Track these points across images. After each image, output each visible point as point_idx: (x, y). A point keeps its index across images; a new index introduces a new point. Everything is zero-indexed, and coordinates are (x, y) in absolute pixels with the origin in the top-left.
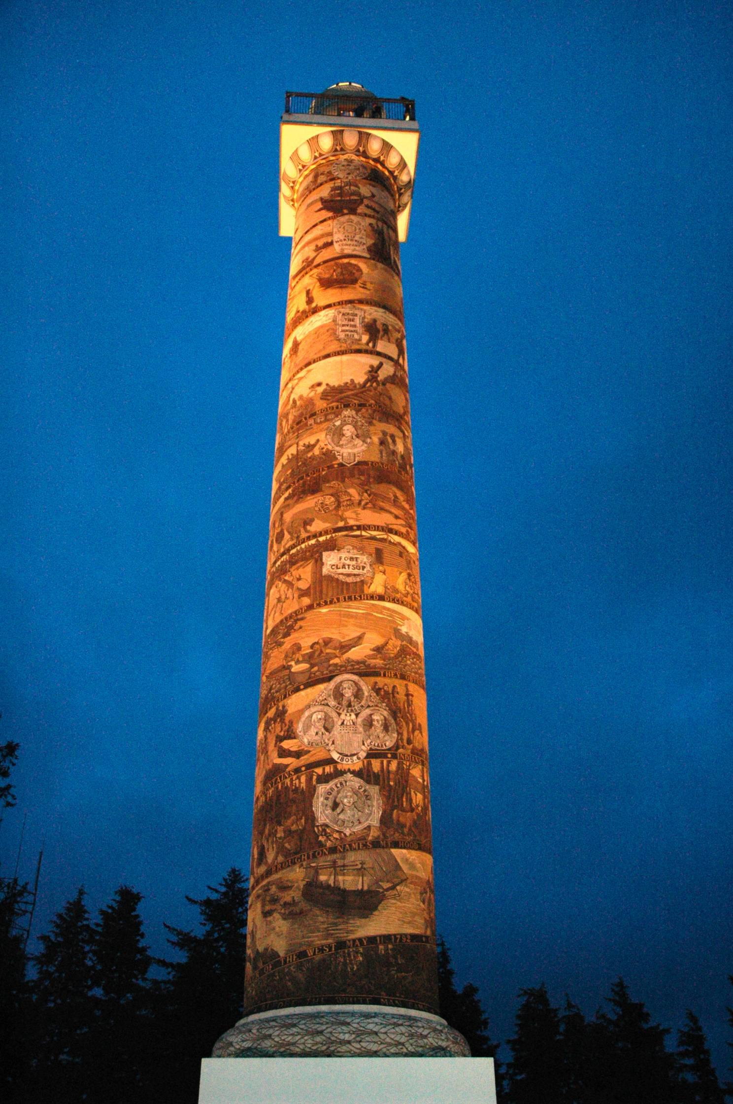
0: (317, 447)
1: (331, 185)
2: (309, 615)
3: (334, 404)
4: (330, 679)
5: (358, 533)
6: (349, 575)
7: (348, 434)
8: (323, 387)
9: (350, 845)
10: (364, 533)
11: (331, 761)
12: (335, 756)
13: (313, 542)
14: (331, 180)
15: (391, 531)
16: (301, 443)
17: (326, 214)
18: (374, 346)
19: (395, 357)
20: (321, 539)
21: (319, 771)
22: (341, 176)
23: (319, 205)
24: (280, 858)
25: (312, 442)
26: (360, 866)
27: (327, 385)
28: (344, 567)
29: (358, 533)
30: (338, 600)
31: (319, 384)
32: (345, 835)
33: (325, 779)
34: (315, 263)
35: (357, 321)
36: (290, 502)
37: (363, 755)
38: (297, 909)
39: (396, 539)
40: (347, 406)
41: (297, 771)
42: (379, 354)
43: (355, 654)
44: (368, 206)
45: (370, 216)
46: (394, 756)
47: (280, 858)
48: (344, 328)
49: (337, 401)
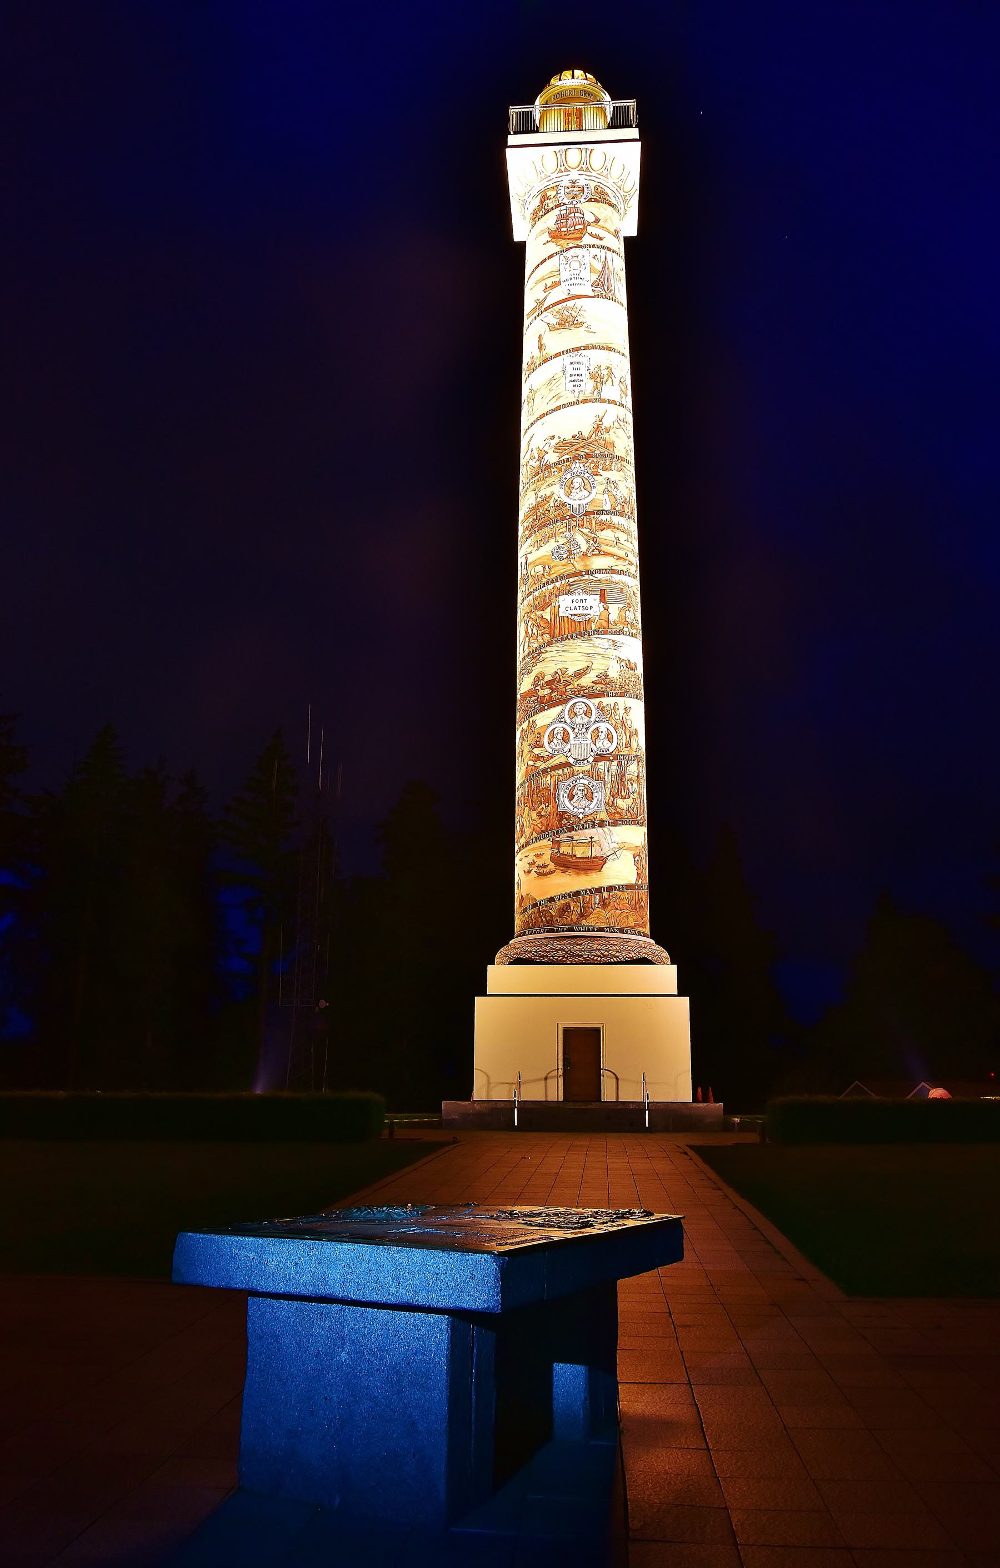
1: (556, 211)
2: (548, 649)
4: (565, 702)
5: (586, 577)
6: (580, 615)
7: (577, 485)
8: (556, 440)
11: (568, 765)
12: (571, 761)
13: (551, 587)
14: (557, 206)
15: (613, 571)
16: (540, 494)
17: (553, 248)
18: (599, 394)
19: (617, 399)
20: (558, 584)
21: (560, 772)
22: (566, 201)
23: (546, 237)
24: (535, 835)
28: (575, 608)
30: (571, 636)
31: (553, 438)
33: (565, 778)
34: (546, 304)
35: (583, 371)
36: (531, 548)
37: (591, 759)
38: (546, 870)
39: (616, 578)
40: (576, 458)
41: (545, 771)
42: (603, 401)
43: (586, 681)
44: (591, 235)
45: (594, 246)
46: (615, 758)
47: (535, 835)
48: (573, 378)
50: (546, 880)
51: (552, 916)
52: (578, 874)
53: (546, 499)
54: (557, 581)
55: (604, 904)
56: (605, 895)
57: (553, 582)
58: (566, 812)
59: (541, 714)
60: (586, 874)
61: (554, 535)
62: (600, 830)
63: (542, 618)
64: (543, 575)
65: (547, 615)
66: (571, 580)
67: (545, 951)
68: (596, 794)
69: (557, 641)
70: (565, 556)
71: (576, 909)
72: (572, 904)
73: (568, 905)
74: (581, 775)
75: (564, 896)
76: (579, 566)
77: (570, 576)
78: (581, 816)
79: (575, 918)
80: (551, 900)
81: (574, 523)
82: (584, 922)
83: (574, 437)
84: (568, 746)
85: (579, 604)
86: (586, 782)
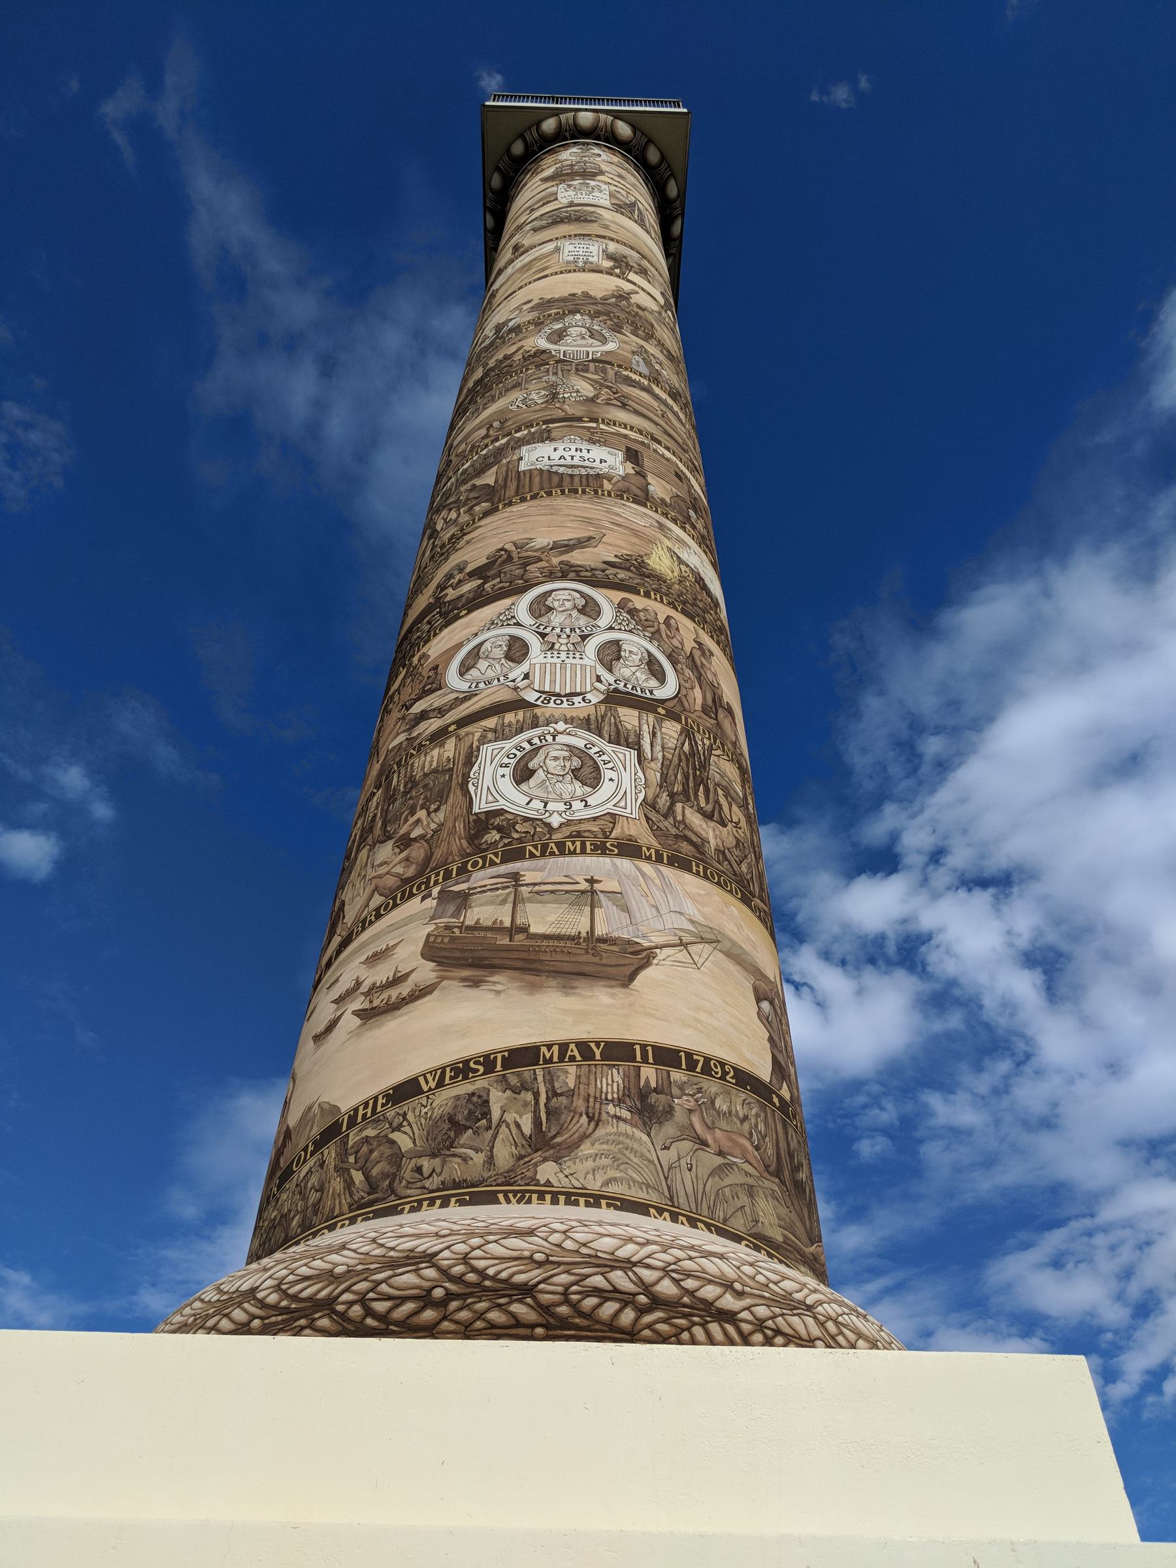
9: (561, 846)
12: (531, 696)
21: (491, 722)
26: (584, 886)
32: (548, 825)
37: (595, 698)
50: (392, 1026)
51: (397, 1157)
52: (533, 988)
55: (647, 1109)
56: (649, 1073)
58: (501, 812)
59: (446, 631)
60: (567, 989)
62: (625, 864)
67: (330, 1276)
68: (608, 774)
71: (513, 1114)
72: (498, 1099)
73: (479, 1106)
74: (561, 726)
75: (462, 1070)
78: (555, 821)
79: (504, 1154)
80: (407, 1090)
82: (547, 1171)
84: (524, 667)
86: (580, 743)
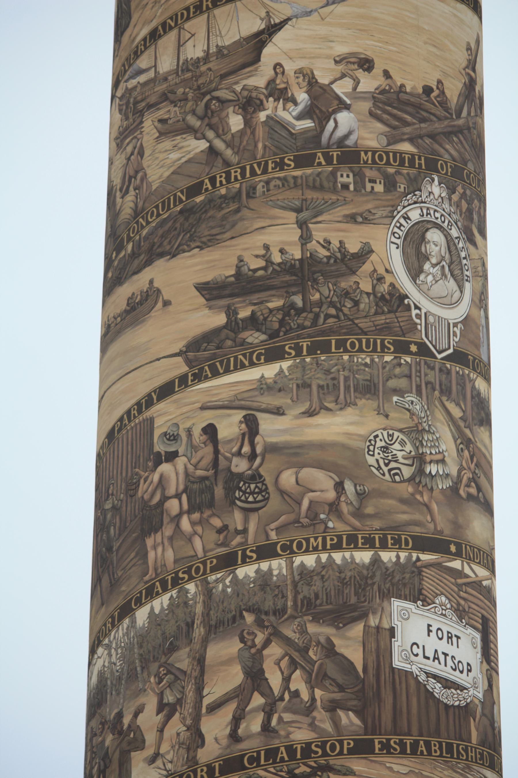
0: (367, 267)
3: (406, 147)
5: (456, 564)
6: (448, 684)
10: (467, 570)
13: (364, 556)
16: (319, 233)
20: (387, 556)
25: (353, 247)
27: (387, 74)
29: (456, 564)
31: (366, 64)
40: (432, 166)
49: (411, 140)
53: (350, 262)
54: (384, 546)
57: (369, 543)
61: (369, 389)
63: (329, 650)
64: (334, 508)
65: (351, 645)
66: (426, 557)
69: (386, 748)
70: (407, 472)
76: (440, 520)
77: (422, 544)
81: (431, 377)
83: (428, 90)
85: (443, 646)
